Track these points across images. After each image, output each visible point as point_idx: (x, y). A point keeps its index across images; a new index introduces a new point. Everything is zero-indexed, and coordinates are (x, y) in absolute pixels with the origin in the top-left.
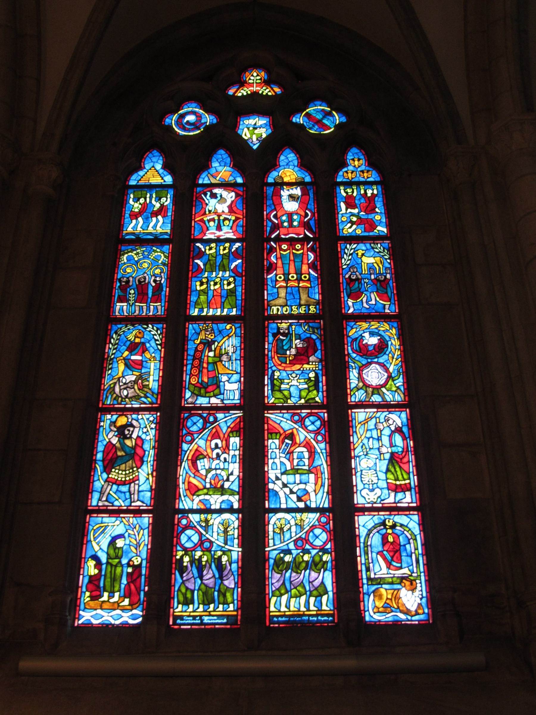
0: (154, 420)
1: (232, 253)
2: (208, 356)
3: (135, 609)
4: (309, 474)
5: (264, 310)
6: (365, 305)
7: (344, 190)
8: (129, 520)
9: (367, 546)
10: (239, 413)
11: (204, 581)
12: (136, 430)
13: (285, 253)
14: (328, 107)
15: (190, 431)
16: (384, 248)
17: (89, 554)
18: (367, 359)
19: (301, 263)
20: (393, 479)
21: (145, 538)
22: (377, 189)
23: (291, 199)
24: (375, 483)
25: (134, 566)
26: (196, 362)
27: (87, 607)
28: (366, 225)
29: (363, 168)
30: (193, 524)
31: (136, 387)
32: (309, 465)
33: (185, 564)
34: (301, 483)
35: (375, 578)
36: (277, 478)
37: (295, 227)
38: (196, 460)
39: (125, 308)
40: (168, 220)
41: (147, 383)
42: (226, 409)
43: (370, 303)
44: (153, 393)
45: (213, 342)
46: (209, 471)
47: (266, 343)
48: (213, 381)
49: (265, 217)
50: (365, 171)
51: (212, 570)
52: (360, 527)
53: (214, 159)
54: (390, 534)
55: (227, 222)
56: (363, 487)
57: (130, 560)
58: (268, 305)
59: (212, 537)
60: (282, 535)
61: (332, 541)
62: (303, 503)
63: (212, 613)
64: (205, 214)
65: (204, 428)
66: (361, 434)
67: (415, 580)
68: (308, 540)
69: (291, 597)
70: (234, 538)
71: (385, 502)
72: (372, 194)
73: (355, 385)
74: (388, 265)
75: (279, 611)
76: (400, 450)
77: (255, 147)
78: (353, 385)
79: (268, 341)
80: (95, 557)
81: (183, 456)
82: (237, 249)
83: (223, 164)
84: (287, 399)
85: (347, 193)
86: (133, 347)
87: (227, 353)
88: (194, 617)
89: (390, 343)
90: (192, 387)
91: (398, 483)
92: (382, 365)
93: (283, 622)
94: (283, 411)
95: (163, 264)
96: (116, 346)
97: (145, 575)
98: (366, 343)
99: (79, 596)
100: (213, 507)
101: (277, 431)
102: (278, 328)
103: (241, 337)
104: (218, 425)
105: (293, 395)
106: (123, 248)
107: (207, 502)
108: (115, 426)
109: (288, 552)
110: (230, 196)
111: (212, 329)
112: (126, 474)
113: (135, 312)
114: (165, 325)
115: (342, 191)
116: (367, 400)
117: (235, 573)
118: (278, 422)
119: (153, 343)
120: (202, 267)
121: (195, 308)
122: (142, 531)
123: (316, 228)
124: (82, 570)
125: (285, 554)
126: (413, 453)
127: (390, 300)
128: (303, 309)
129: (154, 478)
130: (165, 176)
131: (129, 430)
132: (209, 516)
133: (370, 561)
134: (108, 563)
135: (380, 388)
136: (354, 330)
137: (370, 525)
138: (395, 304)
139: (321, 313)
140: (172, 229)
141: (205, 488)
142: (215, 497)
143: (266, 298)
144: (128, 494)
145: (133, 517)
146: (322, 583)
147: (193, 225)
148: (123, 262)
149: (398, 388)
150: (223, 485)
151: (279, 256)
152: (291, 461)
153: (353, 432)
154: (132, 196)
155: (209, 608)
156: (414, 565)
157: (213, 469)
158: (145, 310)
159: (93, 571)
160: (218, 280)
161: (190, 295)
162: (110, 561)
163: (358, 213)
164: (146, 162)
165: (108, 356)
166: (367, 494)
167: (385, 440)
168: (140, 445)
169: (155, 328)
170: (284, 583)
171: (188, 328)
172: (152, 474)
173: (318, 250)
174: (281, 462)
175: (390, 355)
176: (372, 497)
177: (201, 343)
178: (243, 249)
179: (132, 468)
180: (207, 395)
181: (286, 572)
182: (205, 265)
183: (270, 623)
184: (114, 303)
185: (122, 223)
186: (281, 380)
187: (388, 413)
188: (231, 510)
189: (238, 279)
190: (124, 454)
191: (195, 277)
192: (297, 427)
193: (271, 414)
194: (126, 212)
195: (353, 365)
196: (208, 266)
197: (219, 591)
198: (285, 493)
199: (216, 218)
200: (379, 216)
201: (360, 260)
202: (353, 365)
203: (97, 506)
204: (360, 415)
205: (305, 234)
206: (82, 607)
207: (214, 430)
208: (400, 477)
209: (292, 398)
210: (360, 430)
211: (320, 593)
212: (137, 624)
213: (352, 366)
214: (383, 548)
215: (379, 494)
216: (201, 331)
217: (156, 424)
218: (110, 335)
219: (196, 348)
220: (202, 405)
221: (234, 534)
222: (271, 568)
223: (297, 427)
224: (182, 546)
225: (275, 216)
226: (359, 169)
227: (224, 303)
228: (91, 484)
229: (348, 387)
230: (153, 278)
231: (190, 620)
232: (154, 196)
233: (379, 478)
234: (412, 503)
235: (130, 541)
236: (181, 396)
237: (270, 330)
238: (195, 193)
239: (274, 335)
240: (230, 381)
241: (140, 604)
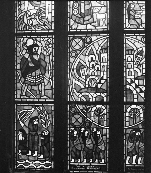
0: (50, 41)
8: (40, 108)
11: (86, 146)
12: (40, 48)
15: (74, 49)
25: (45, 136)
27: (20, 158)
33: (75, 135)
41: (44, 15)
46: (88, 76)
48: (89, 12)
59: (91, 119)
60: (134, 119)
63: (92, 164)
70: (105, 121)
75: (132, 164)
80: (22, 130)
84: (139, 25)
90: (74, 18)
94: (136, 34)
100: (91, 100)
101: (132, 49)
104: (93, 44)
107: (87, 97)
108: (26, 46)
109: (138, 130)
118: (133, 42)
129: (53, 81)
131: (35, 49)
134: (29, 134)
141: (85, 87)
142: (92, 94)
150: (97, 85)
159: (21, 138)
162: (31, 132)
168: (43, 59)
174: (134, 70)
181: (136, 142)
186: (135, 10)
188: (102, 103)
197: (96, 152)
203: (20, 98)
220: (82, 31)
221: (104, 118)
222: (127, 140)
231: (79, 168)
240: (100, 12)
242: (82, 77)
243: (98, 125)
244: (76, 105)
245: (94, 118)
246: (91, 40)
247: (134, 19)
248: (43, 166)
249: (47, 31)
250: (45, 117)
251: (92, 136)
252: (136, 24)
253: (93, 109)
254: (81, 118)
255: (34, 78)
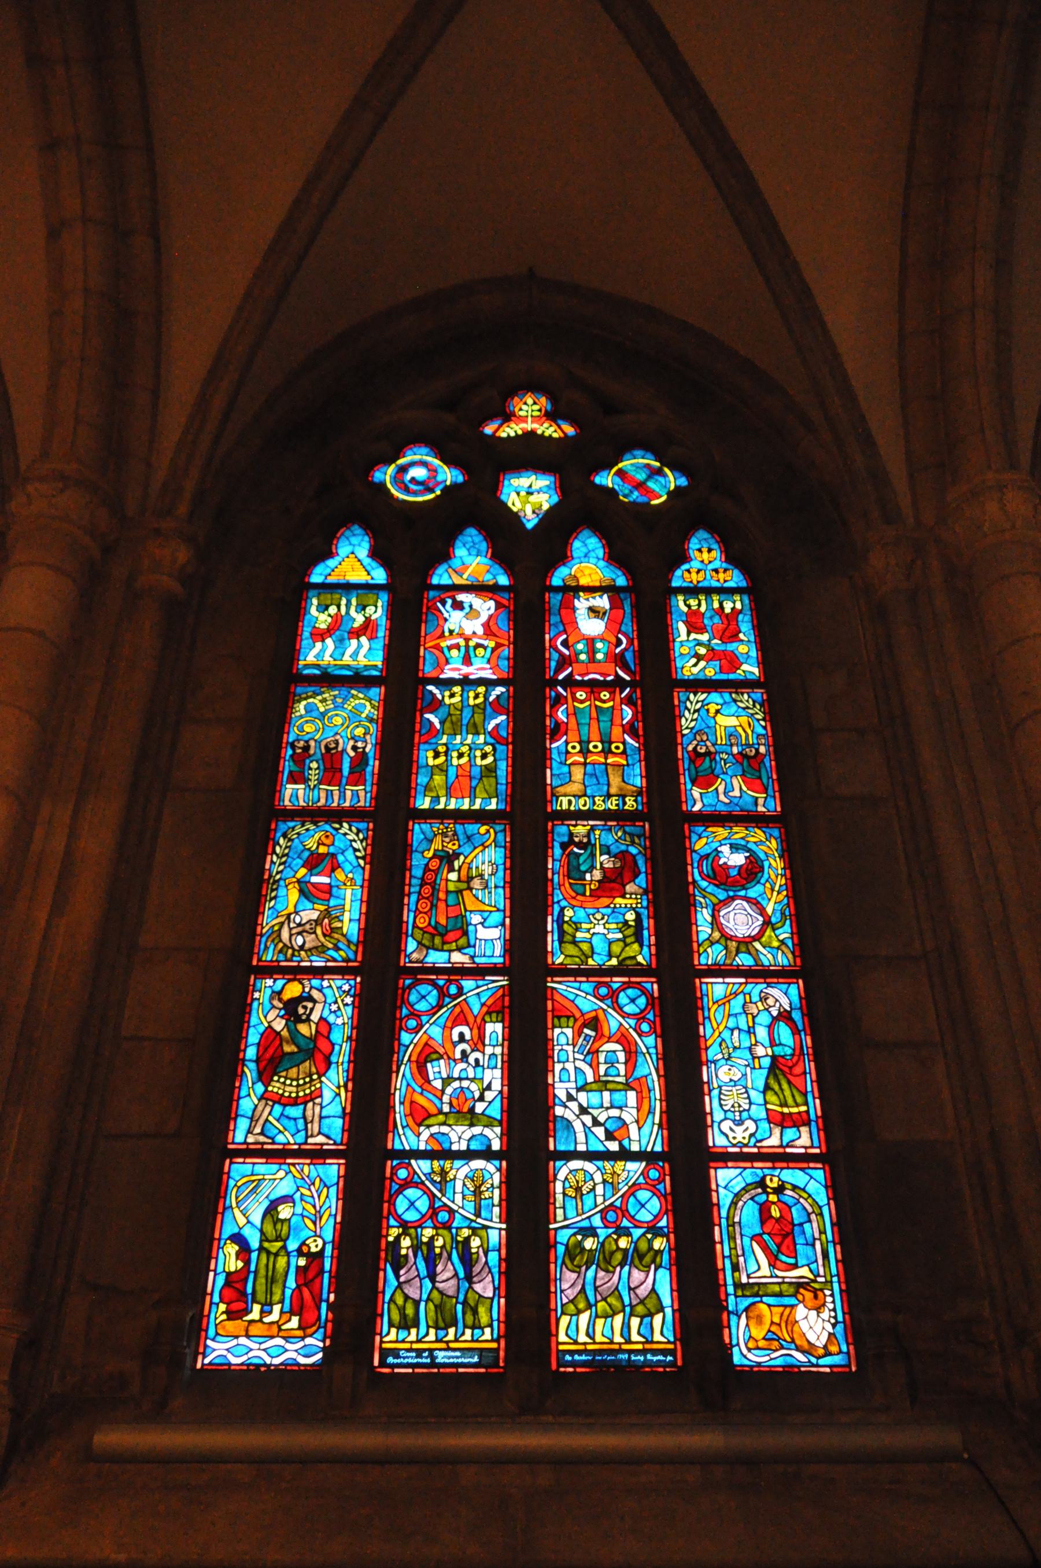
0: (350, 990)
1: (490, 703)
2: (447, 880)
3: (311, 1336)
4: (626, 1091)
5: (545, 802)
6: (722, 797)
7: (685, 601)
9: (733, 1225)
10: (503, 981)
11: (437, 1284)
12: (319, 1007)
13: (581, 706)
14: (656, 460)
16: (754, 702)
17: (229, 1230)
18: (727, 891)
19: (609, 724)
20: (778, 1103)
21: (331, 1202)
22: (741, 600)
23: (592, 615)
24: (744, 1110)
25: (309, 1255)
26: (427, 890)
27: (220, 1332)
28: (723, 661)
29: (717, 564)
30: (419, 1177)
31: (319, 931)
32: (626, 1076)
33: (403, 1252)
34: (612, 1107)
35: (748, 1283)
36: (570, 1098)
37: (599, 662)
38: (426, 1062)
39: (301, 793)
40: (379, 644)
41: (339, 925)
42: (479, 972)
43: (731, 794)
44: (349, 942)
45: (456, 855)
46: (447, 1081)
47: (550, 860)
48: (456, 923)
49: (547, 644)
50: (721, 570)
51: (453, 1264)
52: (721, 1190)
53: (458, 543)
54: (774, 1203)
55: (480, 651)
56: (722, 1117)
57: (303, 1243)
58: (553, 794)
59: (453, 1202)
60: (579, 1201)
61: (670, 1213)
62: (617, 1143)
63: (452, 1345)
64: (442, 636)
65: (439, 1006)
66: (719, 1021)
67: (822, 1290)
68: (627, 1210)
69: (597, 1316)
70: (493, 1205)
71: (765, 1143)
72: (733, 609)
73: (707, 936)
74: (760, 731)
75: (576, 1342)
76: (789, 1051)
77: (530, 525)
78: (703, 937)
79: (553, 856)
80: (238, 1239)
81: (401, 1054)
82: (498, 697)
83: (474, 552)
84: (587, 957)
85: (689, 606)
86: (313, 862)
87: (481, 876)
88: (419, 1352)
89: (766, 864)
90: (418, 934)
91: (786, 1110)
92: (754, 902)
93: (583, 1364)
94: (579, 979)
95: (371, 720)
96: (284, 859)
97: (330, 1272)
98: (725, 863)
99: (206, 1312)
100: (455, 1147)
101: (569, 1014)
102: (571, 835)
103: (505, 847)
105: (596, 950)
106: (299, 690)
108: (280, 1000)
109: (591, 1232)
110: (485, 607)
111: (455, 834)
112: (298, 1086)
113: (319, 800)
114: (371, 825)
115: (680, 602)
116: (728, 962)
117: (495, 1270)
118: (572, 997)
119: (350, 855)
120: (438, 726)
121: (425, 796)
122: (325, 1190)
123: (635, 665)
124: (213, 1262)
125: (585, 1237)
126: (811, 1058)
127: (766, 791)
128: (614, 802)
129: (349, 1094)
130: (373, 569)
131: (305, 1007)
132: (448, 1164)
133: (740, 1252)
134: (261, 1249)
135: (751, 943)
136: (704, 840)
137: (738, 1185)
138: (774, 797)
139: (646, 810)
140: (386, 660)
141: (441, 1112)
142: (459, 1129)
143: (549, 781)
144: (301, 1122)
145: (309, 1164)
146: (653, 1290)
147: (422, 653)
148: (298, 714)
149: (782, 942)
151: (571, 710)
152: (594, 1066)
153: (704, 1018)
154: (315, 601)
155: (447, 1335)
156: (820, 1261)
157: (456, 1079)
158: (336, 798)
159: (234, 1265)
160: (465, 749)
161: (417, 774)
162: (266, 1245)
163: (709, 641)
164: (340, 545)
165: (270, 876)
166: (731, 1129)
167: (762, 1033)
168: (326, 1034)
169: (354, 829)
170: (583, 1288)
171: (412, 830)
172: (346, 1086)
173: (639, 702)
174: (576, 1068)
175: (768, 885)
176: (740, 1134)
177: (434, 856)
178: (509, 697)
179: (310, 1075)
180: (446, 947)
181: (587, 1269)
182: (442, 723)
183: (559, 1366)
184: (282, 785)
185: (298, 647)
186: (575, 923)
187: (765, 985)
188: (487, 1154)
189: (501, 748)
190: (296, 1050)
191: (426, 742)
192: (605, 1007)
193: (559, 983)
194: (305, 629)
195: (702, 900)
196: (448, 725)
197: (465, 1303)
198: (584, 1124)
199: (462, 642)
200: (746, 648)
201: (712, 721)
202: (702, 900)
203: (245, 1143)
204: (717, 988)
205: (617, 675)
206: (211, 1332)
207: (458, 1010)
208: (790, 1101)
209: (595, 956)
210: (717, 1014)
211: (648, 1310)
212: (313, 1365)
213: (701, 903)
214: (762, 1228)
215: (752, 1129)
216: (435, 835)
217: (354, 996)
218: (273, 839)
219: (427, 865)
221: (492, 1198)
222: (559, 1262)
223: (605, 1007)
224: (398, 1218)
225: (565, 643)
226: (711, 567)
227: (475, 789)
228: (235, 1103)
229: (695, 939)
230: (351, 743)
232: (354, 601)
233: (753, 1100)
234: (812, 1147)
235: (304, 1208)
236: (399, 948)
237: (556, 837)
238: (425, 601)
239: (564, 846)
240: (486, 924)
241: (319, 1328)
242: (433, 1083)
243: (473, 1218)
244: (413, 1162)
245: (464, 1198)
246: (460, 989)
247: (574, 942)
248: (294, 1355)
249: (344, 964)
250: (316, 1195)
251: (454, 1252)
252: (579, 954)
253: (461, 1175)
254: (425, 1196)
255: (295, 1083)
